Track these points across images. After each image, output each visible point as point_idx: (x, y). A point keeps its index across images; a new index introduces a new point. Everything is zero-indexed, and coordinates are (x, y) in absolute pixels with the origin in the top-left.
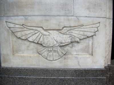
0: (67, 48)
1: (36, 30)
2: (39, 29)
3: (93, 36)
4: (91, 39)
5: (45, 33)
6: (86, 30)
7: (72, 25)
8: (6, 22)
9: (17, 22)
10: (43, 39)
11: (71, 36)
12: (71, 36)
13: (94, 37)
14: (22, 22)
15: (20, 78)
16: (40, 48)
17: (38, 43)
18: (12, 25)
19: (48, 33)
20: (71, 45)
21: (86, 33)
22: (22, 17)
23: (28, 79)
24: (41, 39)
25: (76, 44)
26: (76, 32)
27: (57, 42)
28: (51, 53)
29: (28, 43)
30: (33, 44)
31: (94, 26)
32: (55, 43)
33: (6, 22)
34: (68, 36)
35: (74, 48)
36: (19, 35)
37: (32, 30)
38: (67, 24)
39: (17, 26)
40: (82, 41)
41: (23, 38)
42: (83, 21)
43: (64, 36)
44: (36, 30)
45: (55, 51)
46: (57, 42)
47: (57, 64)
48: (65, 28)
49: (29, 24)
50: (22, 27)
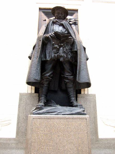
15: (108, 143)
23: (111, 143)
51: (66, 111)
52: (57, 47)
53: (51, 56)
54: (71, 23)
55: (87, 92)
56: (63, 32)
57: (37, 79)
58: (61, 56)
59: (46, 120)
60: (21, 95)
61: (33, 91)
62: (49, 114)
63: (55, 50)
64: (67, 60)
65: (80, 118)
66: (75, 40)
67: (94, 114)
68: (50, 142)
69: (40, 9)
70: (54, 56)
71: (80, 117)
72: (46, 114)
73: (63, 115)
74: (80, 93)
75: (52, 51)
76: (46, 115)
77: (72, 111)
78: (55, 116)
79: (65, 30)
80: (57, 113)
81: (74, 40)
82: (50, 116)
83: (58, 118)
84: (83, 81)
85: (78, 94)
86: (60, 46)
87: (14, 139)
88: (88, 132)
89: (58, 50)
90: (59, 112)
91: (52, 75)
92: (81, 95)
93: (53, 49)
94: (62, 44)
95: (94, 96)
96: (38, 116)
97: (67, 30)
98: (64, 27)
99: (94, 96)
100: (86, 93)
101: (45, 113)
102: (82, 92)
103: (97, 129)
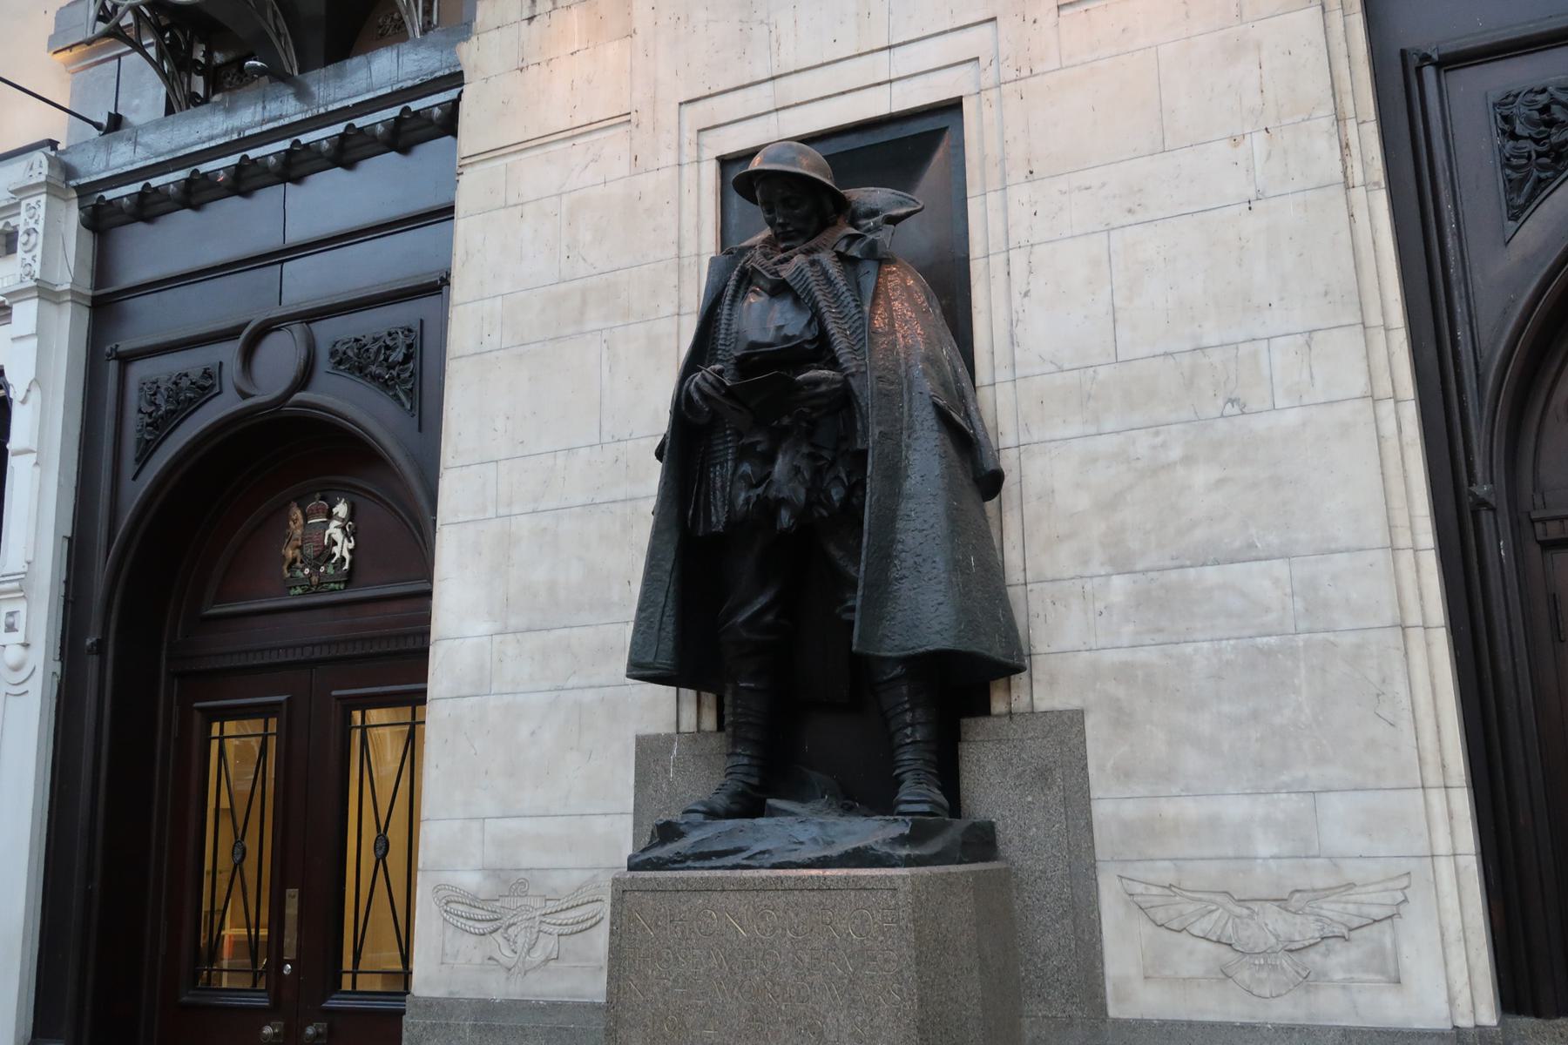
0: (1314, 957)
1: (1214, 903)
2: (1219, 899)
3: (1390, 917)
4: (1387, 923)
5: (1238, 910)
6: (1363, 898)
7: (1319, 884)
8: (1121, 877)
9: (1152, 877)
10: (1235, 927)
11: (1319, 918)
12: (1319, 918)
13: (1396, 919)
14: (1169, 878)
16: (1228, 956)
17: (1219, 942)
18: (1139, 888)
19: (1245, 912)
20: (1322, 948)
21: (1365, 910)
22: (1167, 864)
24: (1229, 930)
25: (1338, 945)
26: (1333, 906)
27: (1277, 937)
28: (1264, 975)
29: (1192, 941)
30: (1204, 944)
31: (1390, 885)
32: (1273, 941)
33: (1121, 877)
34: (1311, 918)
35: (1334, 961)
36: (1160, 915)
37: (1200, 900)
38: (1302, 882)
39: (1154, 890)
40: (1353, 934)
41: (1175, 925)
42: (1351, 871)
43: (1298, 919)
44: (1214, 903)
45: (1274, 967)
46: (1277, 937)
47: (1285, 1010)
48: (1298, 895)
49: (1188, 884)
50: (1167, 892)
51: (802, 843)
52: (758, 442)
53: (732, 504)
54: (855, 251)
55: (1025, 699)
56: (787, 339)
57: (649, 659)
58: (781, 502)
59: (684, 896)
60: (648, 751)
61: (710, 722)
62: (707, 864)
63: (746, 468)
64: (825, 514)
65: (863, 883)
66: (851, 380)
67: (1070, 852)
68: (704, 1026)
69: (725, 162)
70: (747, 500)
71: (859, 878)
72: (689, 863)
73: (774, 867)
74: (984, 710)
75: (734, 473)
76: (689, 868)
77: (830, 844)
78: (728, 873)
79: (804, 319)
80: (745, 855)
81: (845, 381)
82: (706, 873)
83: (743, 887)
84: (910, 644)
85: (965, 721)
86: (778, 437)
87: (595, 1007)
88: (906, 974)
89: (770, 459)
90: (762, 848)
91: (769, 618)
92: (982, 720)
93: (738, 461)
94: (786, 421)
95: (1076, 719)
96: (644, 880)
97: (817, 317)
98: (797, 300)
99: (1076, 719)
100: (1020, 701)
101: (686, 858)
102: (998, 706)
103: (1099, 956)
